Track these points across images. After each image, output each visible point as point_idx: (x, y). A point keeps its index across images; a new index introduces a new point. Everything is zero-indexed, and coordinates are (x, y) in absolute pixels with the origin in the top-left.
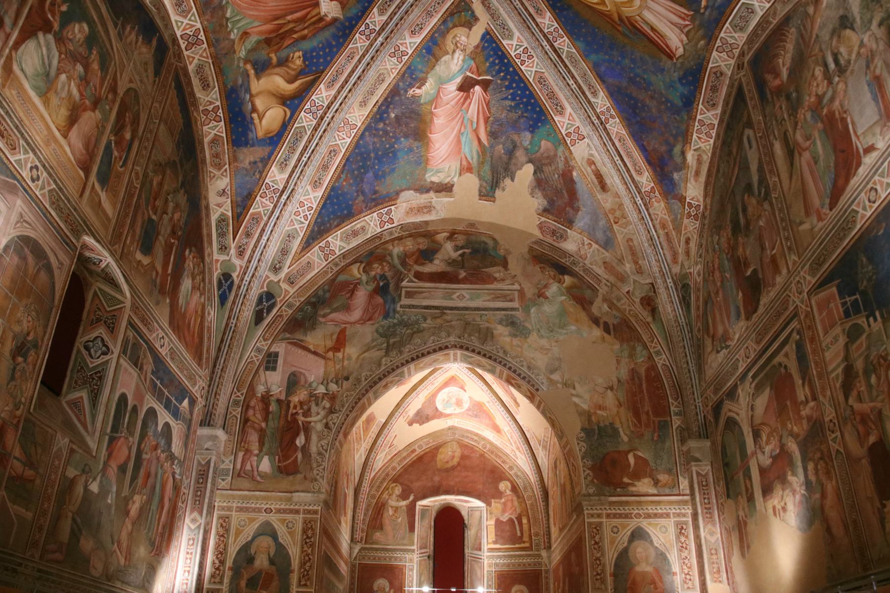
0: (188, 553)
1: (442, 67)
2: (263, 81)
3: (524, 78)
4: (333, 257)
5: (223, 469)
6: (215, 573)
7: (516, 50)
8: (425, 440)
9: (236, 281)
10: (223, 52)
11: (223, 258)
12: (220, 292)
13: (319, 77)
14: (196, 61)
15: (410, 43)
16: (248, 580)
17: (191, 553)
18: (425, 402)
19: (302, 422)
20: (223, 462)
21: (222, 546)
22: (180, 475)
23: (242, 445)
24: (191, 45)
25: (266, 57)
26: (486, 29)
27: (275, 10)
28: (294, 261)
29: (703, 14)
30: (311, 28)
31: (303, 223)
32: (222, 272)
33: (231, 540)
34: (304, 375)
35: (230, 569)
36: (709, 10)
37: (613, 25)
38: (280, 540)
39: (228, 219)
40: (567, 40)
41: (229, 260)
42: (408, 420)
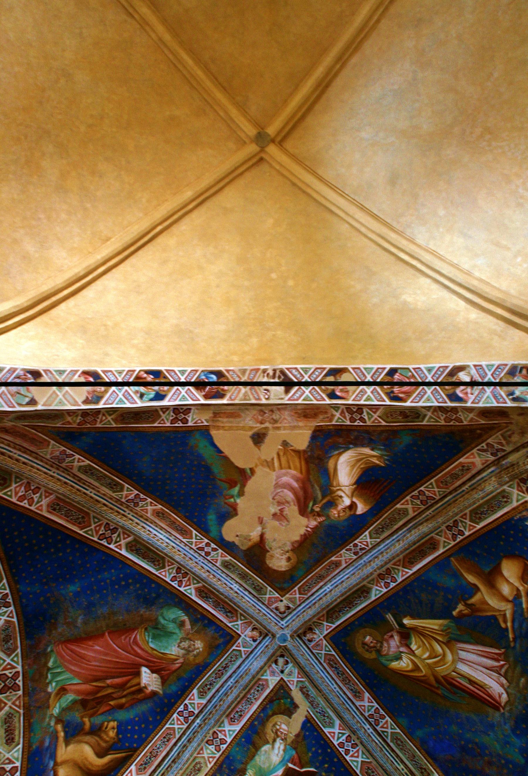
1: (263, 758)
2: (71, 747)
3: (351, 770)
7: (338, 738)
10: (38, 705)
13: (132, 756)
14: (7, 708)
15: (229, 731)
24: (6, 688)
25: (79, 720)
26: (306, 717)
27: (96, 671)
29: (514, 648)
30: (129, 698)
36: (518, 641)
37: (431, 691)
40: (389, 720)
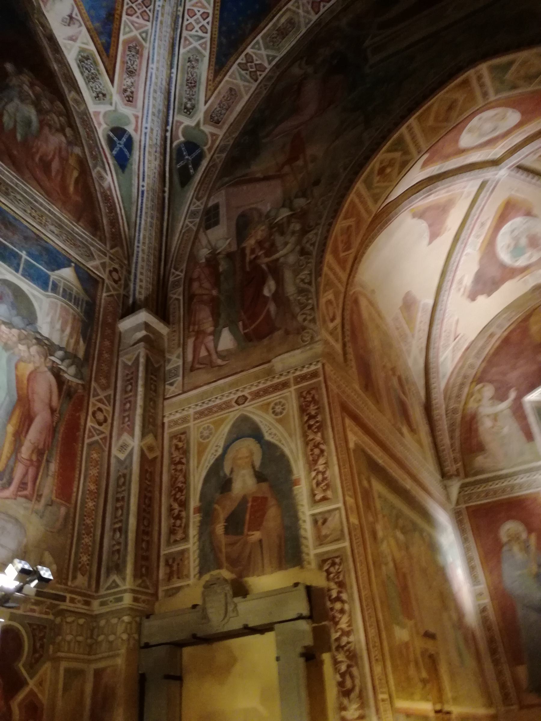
0: (118, 500)
4: (264, 74)
5: (170, 371)
6: (174, 526)
8: (504, 316)
9: (136, 137)
11: (103, 108)
12: (114, 152)
16: (227, 520)
17: (123, 498)
18: (482, 259)
19: (267, 264)
20: (169, 361)
21: (181, 478)
22: (75, 376)
23: (191, 330)
28: (209, 93)
31: (202, 38)
32: (109, 128)
33: (193, 463)
34: (256, 209)
35: (198, 510)
38: (267, 437)
39: (92, 55)
41: (115, 110)
42: (467, 293)
